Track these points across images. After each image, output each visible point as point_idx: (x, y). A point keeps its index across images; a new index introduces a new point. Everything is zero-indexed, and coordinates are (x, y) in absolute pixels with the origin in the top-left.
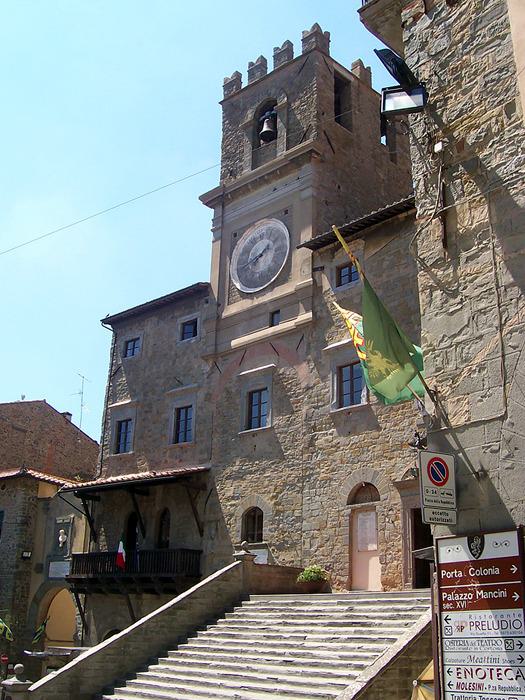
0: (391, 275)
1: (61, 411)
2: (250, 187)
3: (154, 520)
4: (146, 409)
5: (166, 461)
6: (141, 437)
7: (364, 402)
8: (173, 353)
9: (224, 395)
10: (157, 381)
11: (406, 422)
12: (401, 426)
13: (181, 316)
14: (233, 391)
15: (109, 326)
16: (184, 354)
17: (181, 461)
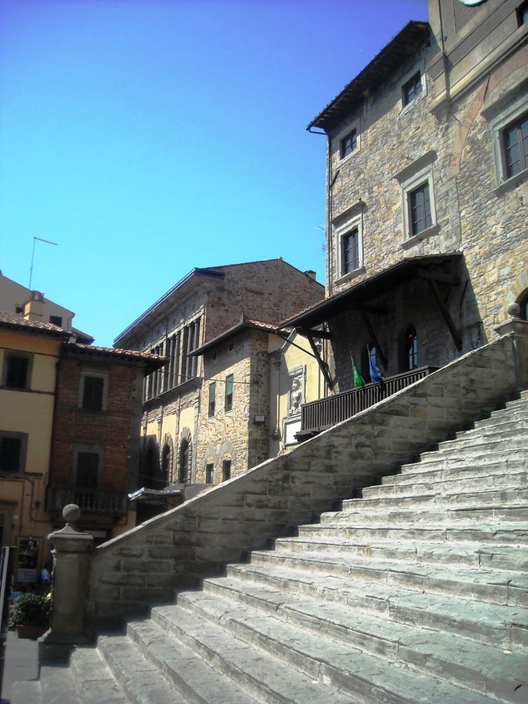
1: (303, 269)
15: (322, 131)
16: (410, 121)
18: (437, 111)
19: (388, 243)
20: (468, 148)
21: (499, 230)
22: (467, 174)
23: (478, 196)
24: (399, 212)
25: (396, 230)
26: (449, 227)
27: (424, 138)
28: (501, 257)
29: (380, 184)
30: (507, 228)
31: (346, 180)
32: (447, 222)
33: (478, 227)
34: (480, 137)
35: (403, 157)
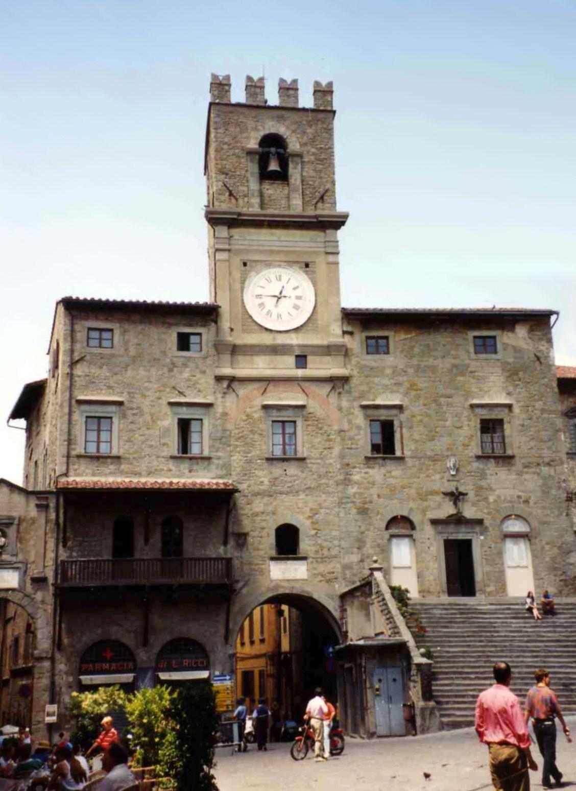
0: (422, 361)
2: (266, 223)
3: (159, 529)
4: (135, 411)
5: (170, 470)
6: (129, 440)
7: (398, 453)
8: (168, 360)
9: (244, 418)
10: (146, 384)
11: (438, 476)
12: (433, 477)
13: (176, 325)
14: (256, 416)
16: (185, 365)
17: (190, 471)
18: (219, 379)
19: (151, 446)
20: (244, 418)
21: (266, 482)
22: (241, 435)
23: (249, 453)
24: (167, 430)
25: (163, 441)
26: (221, 462)
27: (198, 386)
28: (266, 499)
29: (144, 396)
30: (274, 481)
31: (94, 371)
32: (219, 458)
33: (247, 473)
34: (256, 416)
35: (174, 388)
